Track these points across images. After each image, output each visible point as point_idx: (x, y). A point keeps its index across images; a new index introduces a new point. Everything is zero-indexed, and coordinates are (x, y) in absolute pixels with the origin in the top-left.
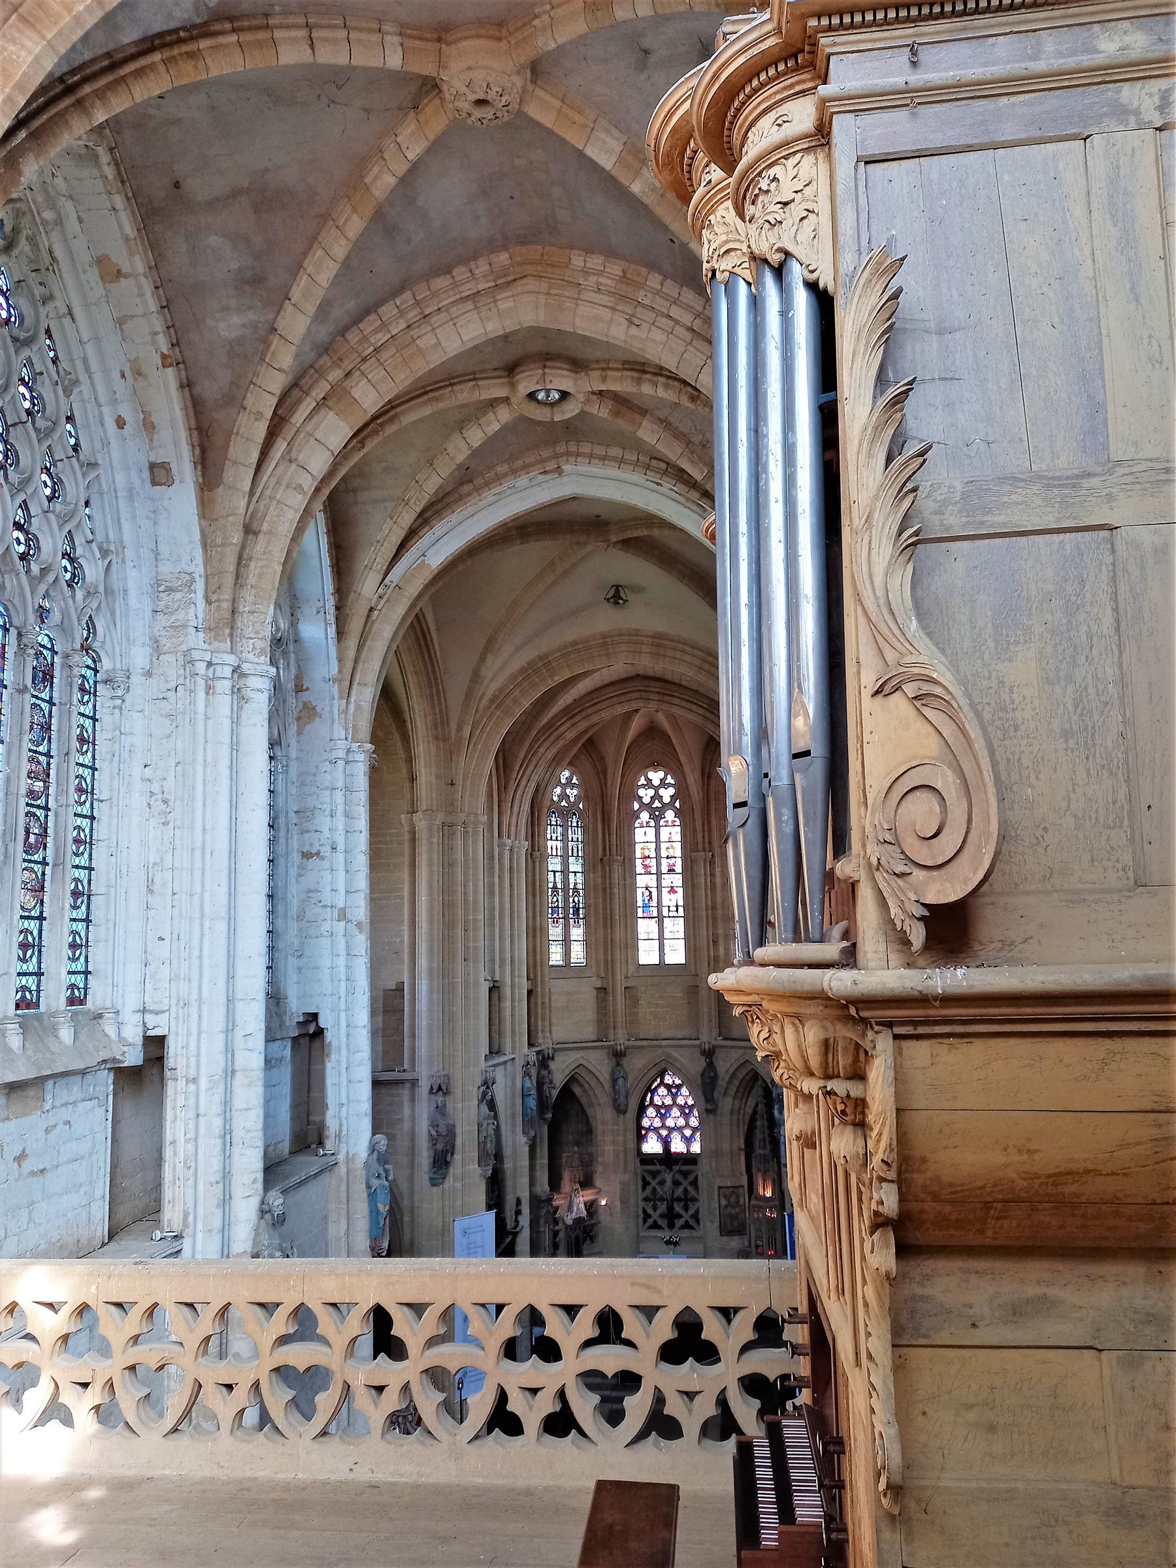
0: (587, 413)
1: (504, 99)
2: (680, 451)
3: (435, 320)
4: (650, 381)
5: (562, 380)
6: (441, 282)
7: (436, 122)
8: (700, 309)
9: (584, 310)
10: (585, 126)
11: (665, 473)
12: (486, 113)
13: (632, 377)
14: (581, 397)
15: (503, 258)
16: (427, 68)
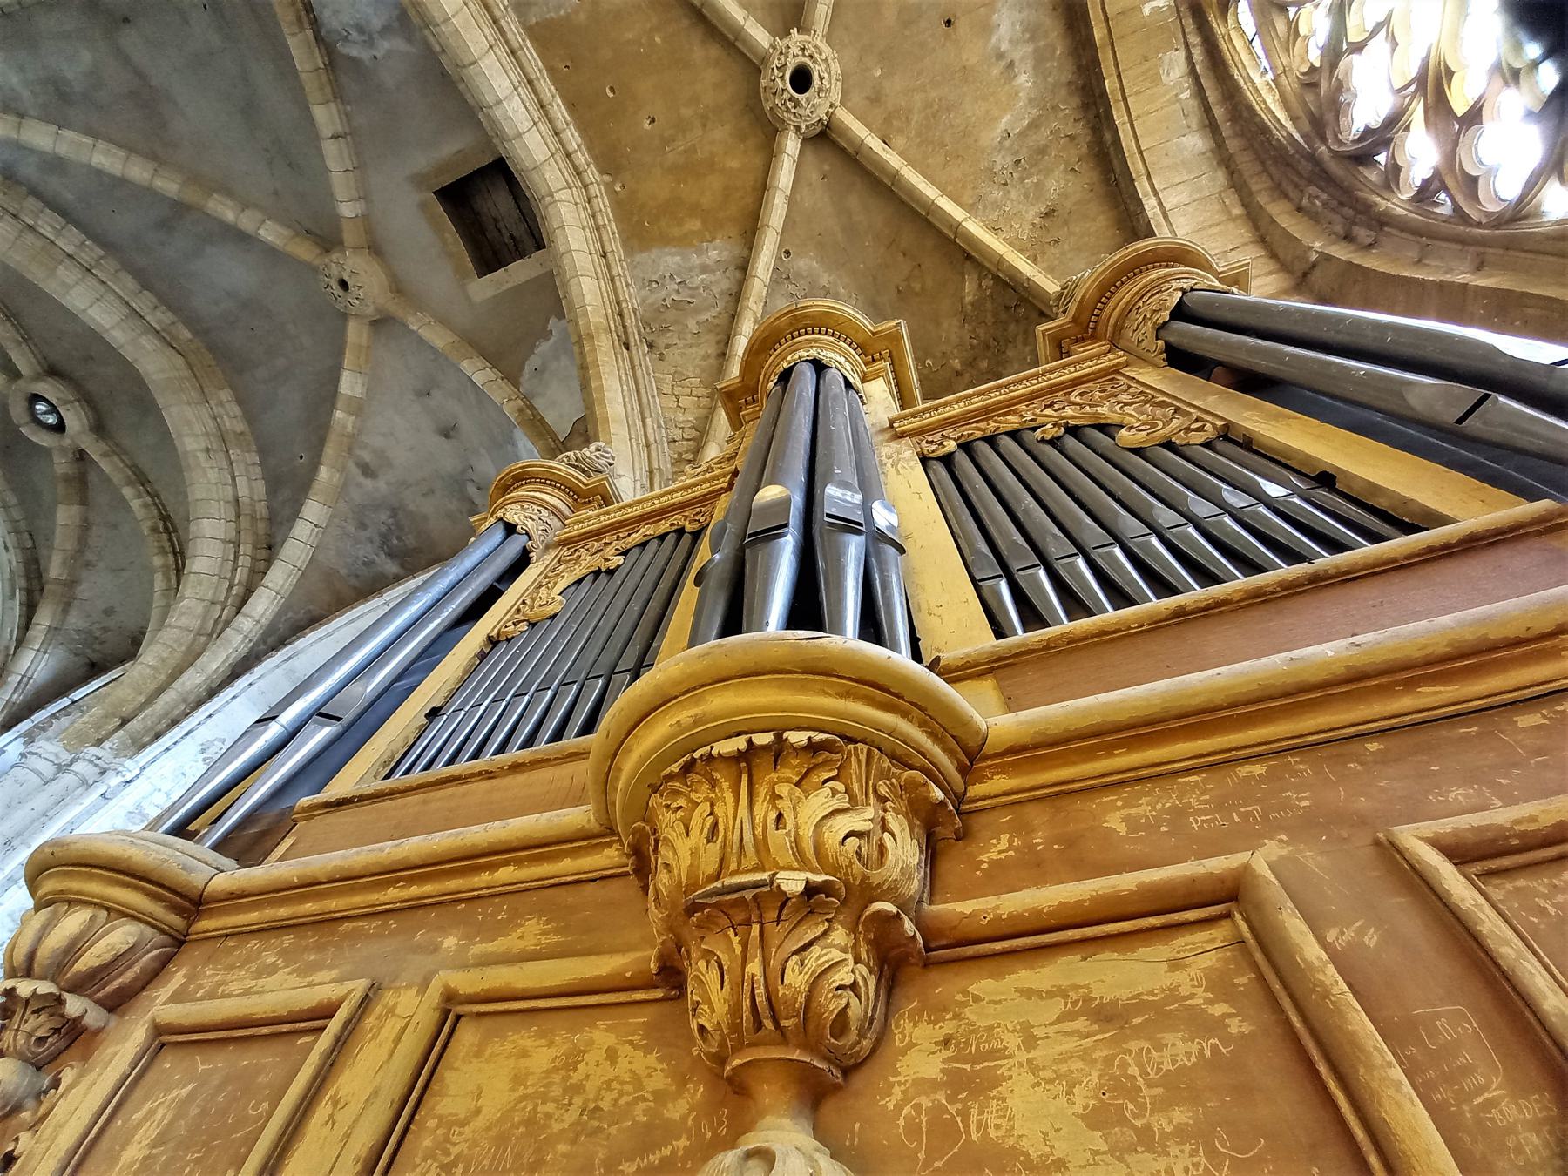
0: (51, 456)
1: (356, 301)
2: (69, 548)
3: (90, 280)
4: (139, 491)
5: (75, 420)
6: (130, 282)
7: (304, 251)
8: (256, 498)
9: (189, 412)
10: (360, 367)
11: (23, 549)
12: (337, 290)
13: (128, 477)
14: (67, 442)
15: (186, 334)
16: (349, 237)
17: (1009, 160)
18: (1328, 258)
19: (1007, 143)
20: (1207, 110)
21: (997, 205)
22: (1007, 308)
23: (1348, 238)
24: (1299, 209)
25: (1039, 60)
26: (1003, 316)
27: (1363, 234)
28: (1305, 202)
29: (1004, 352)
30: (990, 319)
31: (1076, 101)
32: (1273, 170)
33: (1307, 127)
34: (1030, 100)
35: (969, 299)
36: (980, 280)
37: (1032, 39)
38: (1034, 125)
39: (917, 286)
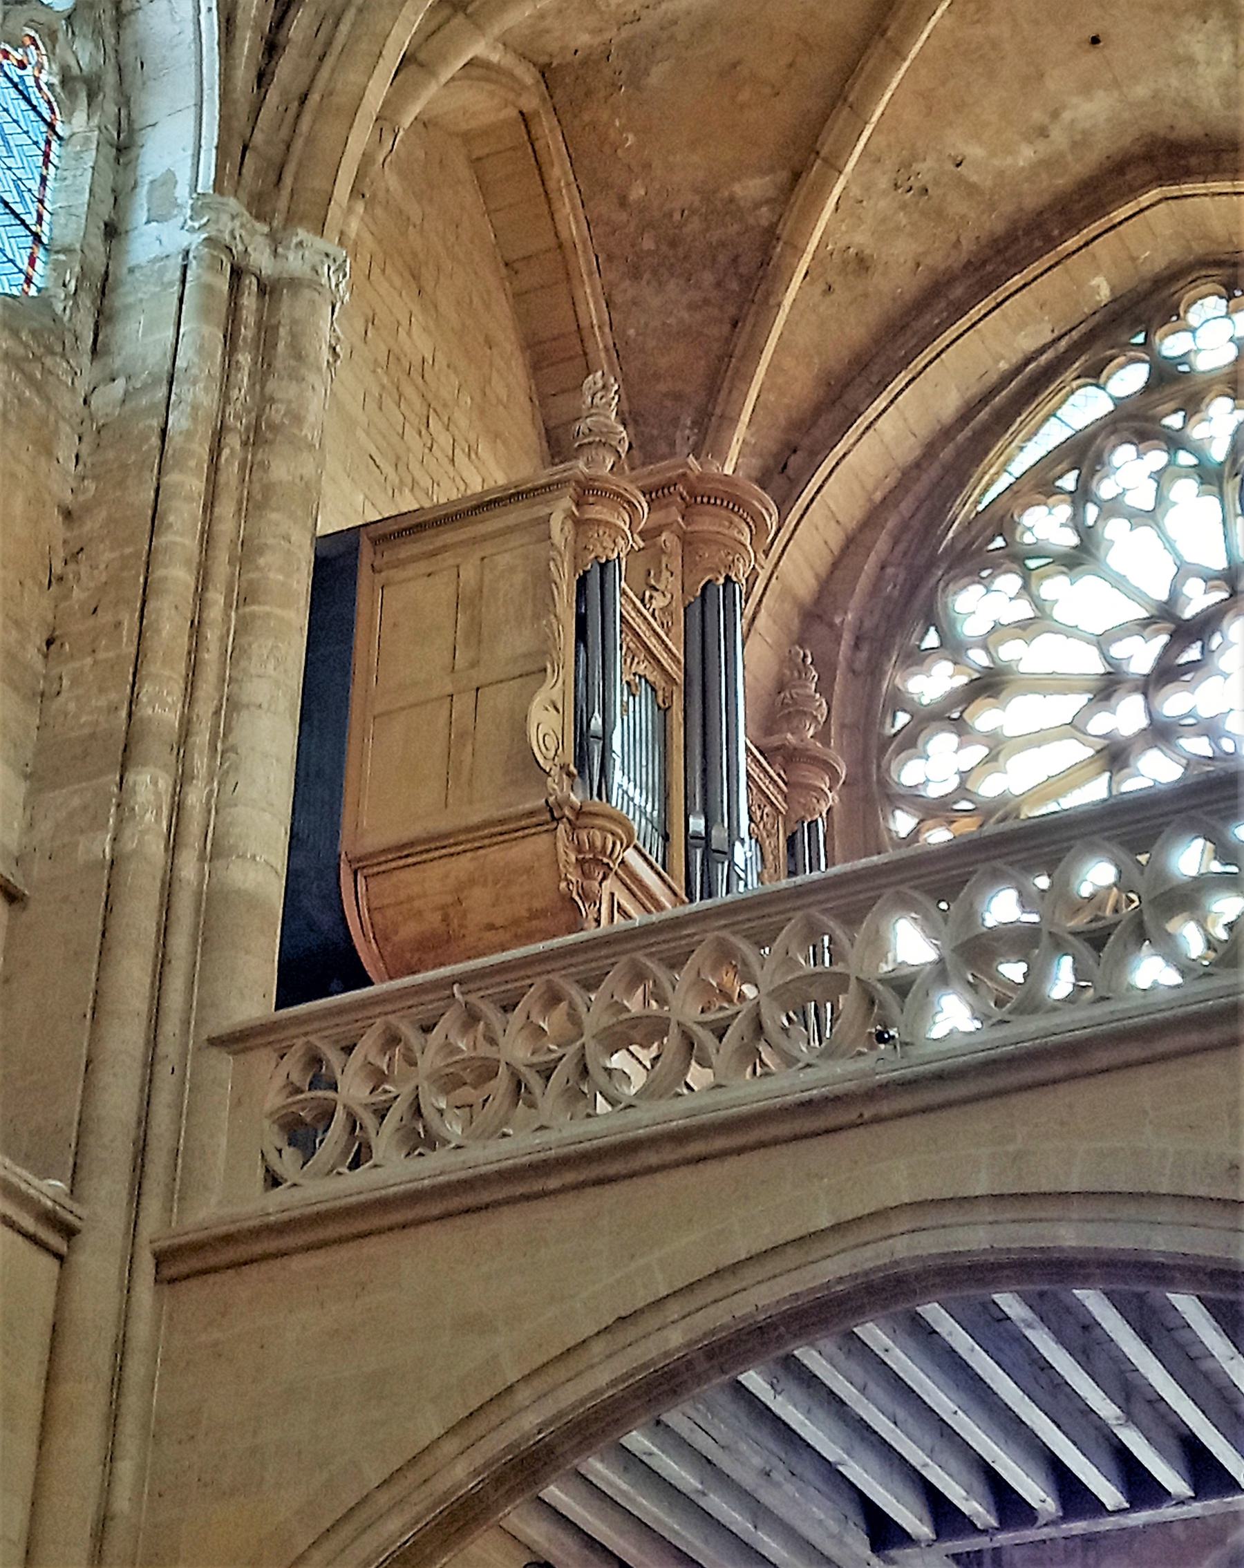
17: (925, 179)
18: (838, 639)
19: (950, 166)
20: (985, 399)
21: (867, 188)
22: (735, 260)
23: (856, 646)
24: (883, 568)
25: (1048, 164)
26: (722, 259)
27: (863, 655)
28: (890, 571)
29: (672, 275)
30: (715, 236)
31: (1000, 228)
32: (920, 515)
33: (960, 546)
34: (1001, 174)
35: (737, 188)
36: (768, 201)
37: (1074, 145)
38: (972, 190)
39: (744, 96)
